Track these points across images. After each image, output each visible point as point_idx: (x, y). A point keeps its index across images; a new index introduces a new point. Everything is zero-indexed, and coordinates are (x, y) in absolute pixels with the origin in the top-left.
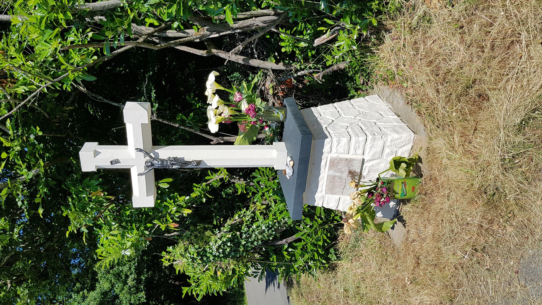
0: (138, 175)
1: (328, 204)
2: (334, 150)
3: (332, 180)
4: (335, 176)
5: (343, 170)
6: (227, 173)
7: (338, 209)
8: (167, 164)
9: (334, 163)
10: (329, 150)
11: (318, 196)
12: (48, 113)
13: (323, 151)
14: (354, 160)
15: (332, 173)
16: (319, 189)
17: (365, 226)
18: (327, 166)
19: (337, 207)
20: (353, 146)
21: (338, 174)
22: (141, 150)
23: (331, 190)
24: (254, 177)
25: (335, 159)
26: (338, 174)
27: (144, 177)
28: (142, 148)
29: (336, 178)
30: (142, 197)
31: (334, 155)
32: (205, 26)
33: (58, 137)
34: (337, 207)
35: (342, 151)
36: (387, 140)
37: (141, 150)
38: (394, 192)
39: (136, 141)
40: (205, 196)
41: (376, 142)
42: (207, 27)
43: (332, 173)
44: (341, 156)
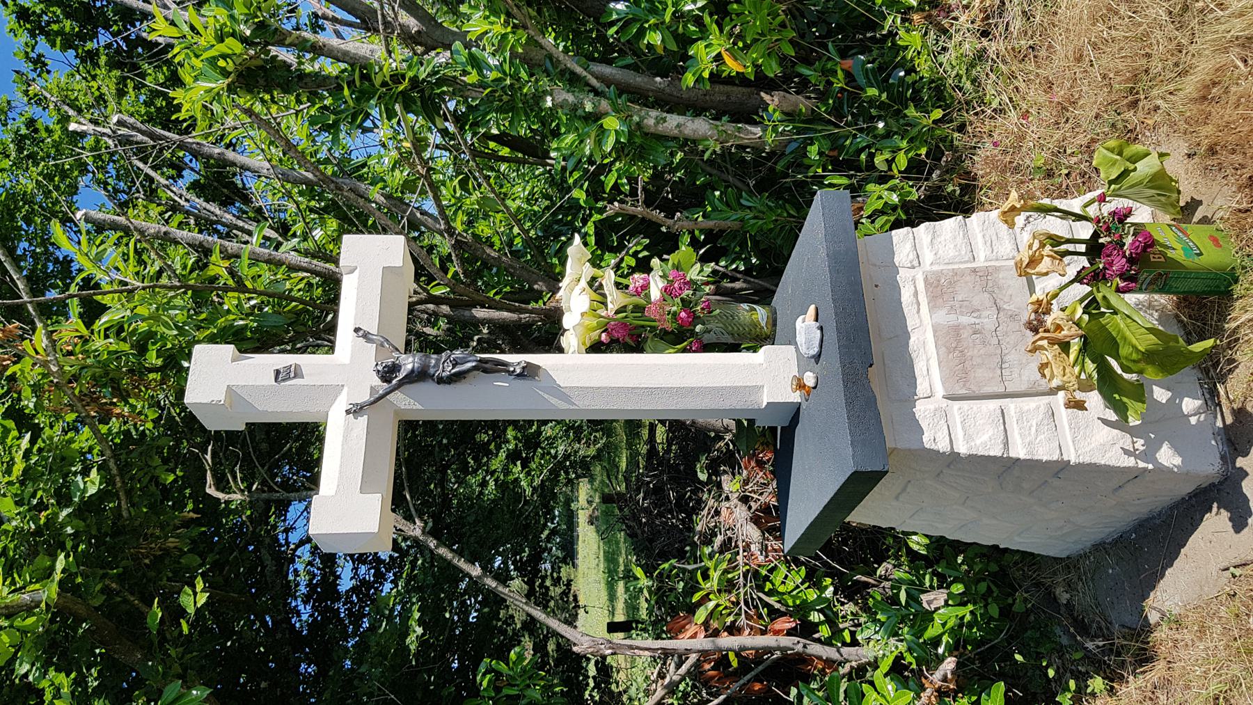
1: (968, 437)
3: (952, 342)
4: (956, 330)
5: (976, 302)
9: (940, 288)
11: (922, 410)
13: (896, 260)
14: (997, 269)
15: (943, 317)
16: (922, 388)
18: (923, 298)
19: (1006, 444)
20: (980, 237)
21: (965, 320)
22: (366, 336)
26: (965, 320)
27: (363, 420)
28: (374, 330)
29: (965, 334)
34: (1006, 444)
35: (952, 253)
37: (366, 336)
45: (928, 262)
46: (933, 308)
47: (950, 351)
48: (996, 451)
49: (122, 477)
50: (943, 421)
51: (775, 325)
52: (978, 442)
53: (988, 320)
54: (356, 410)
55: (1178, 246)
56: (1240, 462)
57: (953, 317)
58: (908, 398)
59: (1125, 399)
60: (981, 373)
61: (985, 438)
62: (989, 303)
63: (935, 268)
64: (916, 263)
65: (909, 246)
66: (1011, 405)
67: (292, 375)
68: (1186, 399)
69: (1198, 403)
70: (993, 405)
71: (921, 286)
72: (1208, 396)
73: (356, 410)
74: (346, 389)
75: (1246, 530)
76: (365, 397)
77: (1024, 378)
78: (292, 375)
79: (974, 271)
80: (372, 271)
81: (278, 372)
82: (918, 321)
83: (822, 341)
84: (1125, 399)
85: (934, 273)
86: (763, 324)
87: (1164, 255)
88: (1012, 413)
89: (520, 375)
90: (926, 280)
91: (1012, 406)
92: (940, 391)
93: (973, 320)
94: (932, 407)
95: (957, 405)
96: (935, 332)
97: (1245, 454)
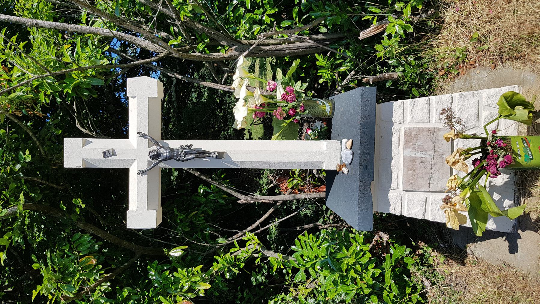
0: (138, 174)
1: (409, 209)
2: (408, 118)
3: (411, 164)
4: (414, 159)
5: (426, 147)
6: (258, 242)
7: (426, 218)
8: (178, 153)
9: (411, 137)
10: (401, 117)
11: (392, 195)
12: (45, 151)
15: (409, 153)
16: (394, 184)
17: (477, 224)
19: (424, 214)
20: (435, 109)
21: (419, 155)
22: (144, 136)
23: (412, 187)
24: (293, 252)
25: (411, 130)
26: (419, 155)
27: (145, 177)
28: (147, 133)
29: (417, 162)
30: (142, 212)
31: (408, 125)
32: (234, 45)
33: (52, 187)
34: (424, 214)
35: (420, 118)
36: (481, 97)
37: (144, 136)
38: (513, 152)
39: (139, 123)
40: (230, 271)
41: (466, 102)
42: (235, 47)
43: (409, 153)
44: (420, 126)
45: (408, 122)
46: (406, 147)
47: (409, 169)
48: (419, 217)
49: (39, 141)
50: (400, 201)
51: (333, 113)
52: (413, 212)
53: (429, 156)
54: (141, 173)
55: (523, 154)
56: (520, 231)
57: (414, 153)
58: (387, 189)
59: (478, 222)
60: (421, 182)
61: (416, 210)
62: (431, 148)
63: (411, 126)
64: (402, 121)
65: (400, 112)
66: (431, 196)
67: (111, 154)
68: (506, 200)
69: (512, 202)
70: (422, 195)
71: (402, 134)
72: (516, 199)
73: (141, 173)
74: (136, 162)
75: (513, 255)
76: (145, 167)
77: (439, 185)
78: (111, 154)
79: (429, 129)
80: (143, 94)
81: (104, 153)
82: (397, 152)
83: (352, 159)
84: (478, 222)
85: (409, 129)
86: (328, 112)
87: (515, 159)
88: (430, 199)
89: (217, 157)
90: (405, 132)
91: (431, 197)
92: (401, 187)
93: (422, 156)
94: (396, 194)
95: (407, 194)
96: (404, 159)
97: (523, 231)
